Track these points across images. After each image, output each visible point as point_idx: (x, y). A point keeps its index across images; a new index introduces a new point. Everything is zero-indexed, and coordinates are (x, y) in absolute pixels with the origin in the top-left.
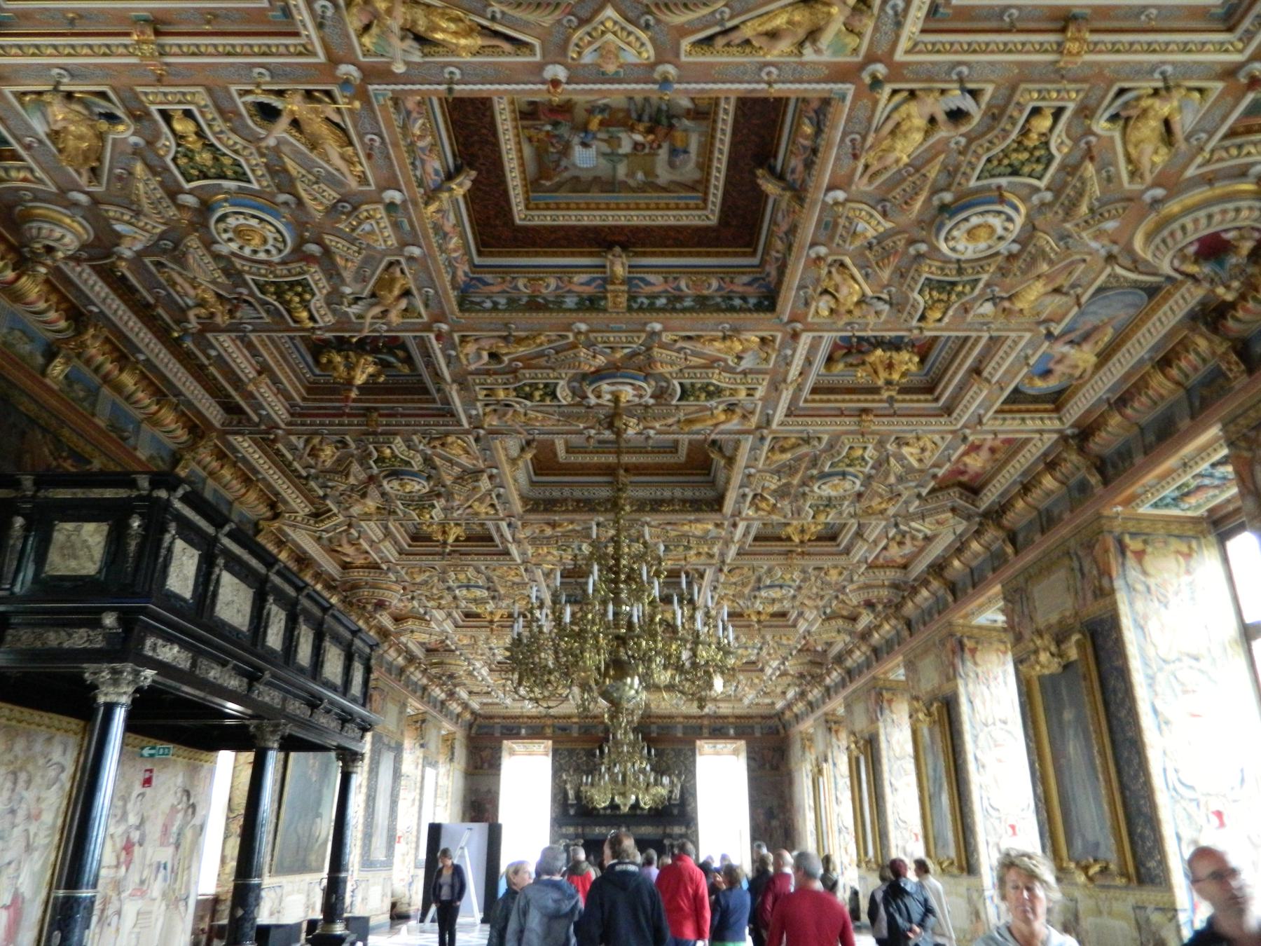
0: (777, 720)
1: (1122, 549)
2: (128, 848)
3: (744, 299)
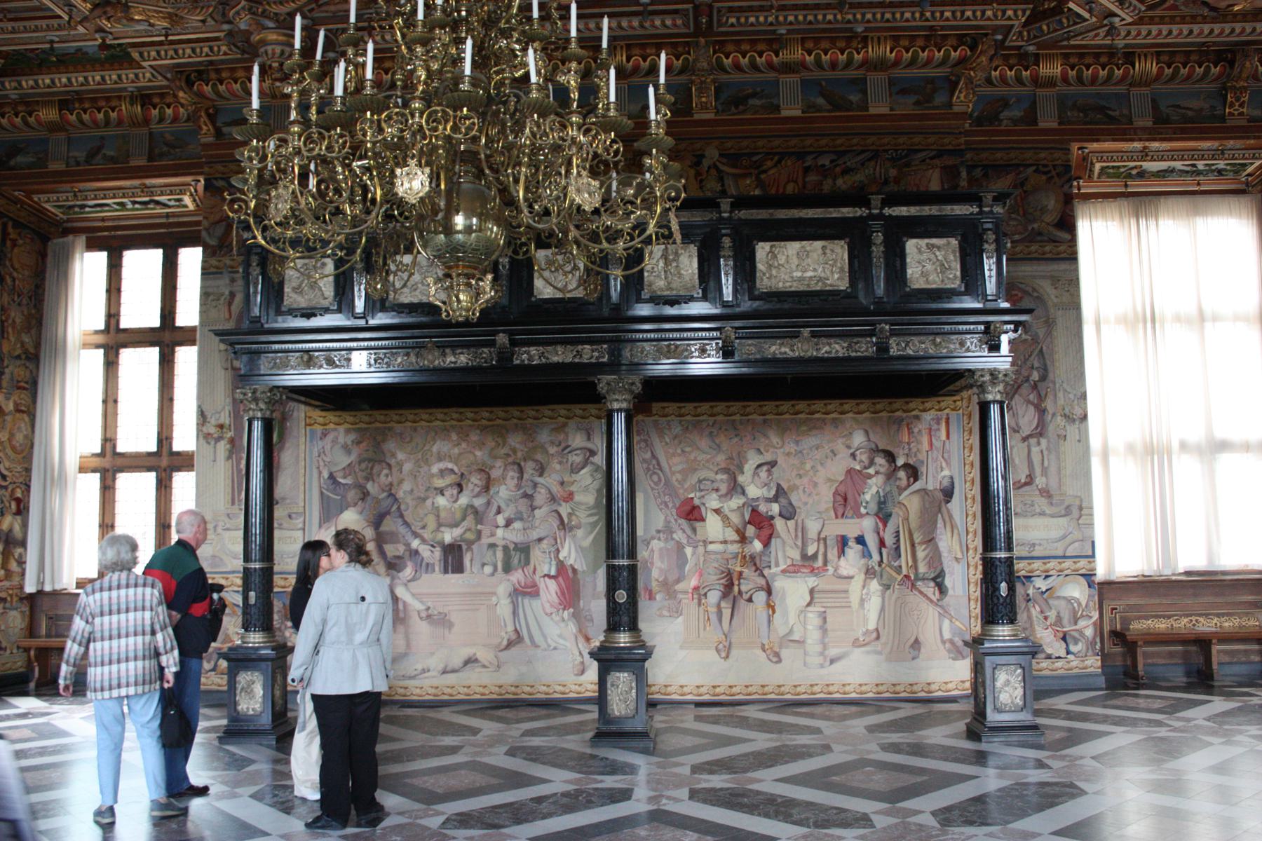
2: (760, 522)
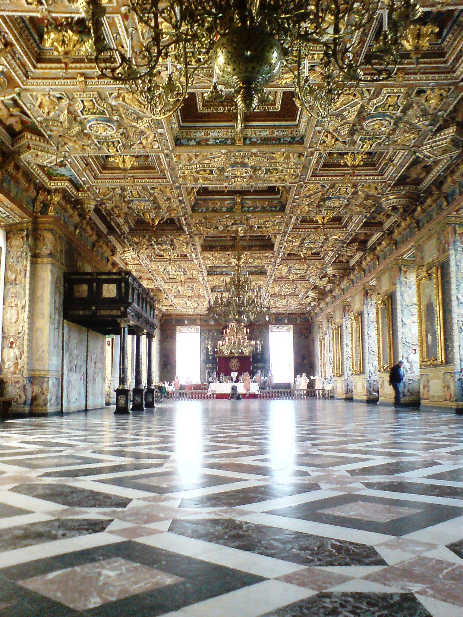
0: (307, 315)
1: (400, 270)
3: (276, 207)
